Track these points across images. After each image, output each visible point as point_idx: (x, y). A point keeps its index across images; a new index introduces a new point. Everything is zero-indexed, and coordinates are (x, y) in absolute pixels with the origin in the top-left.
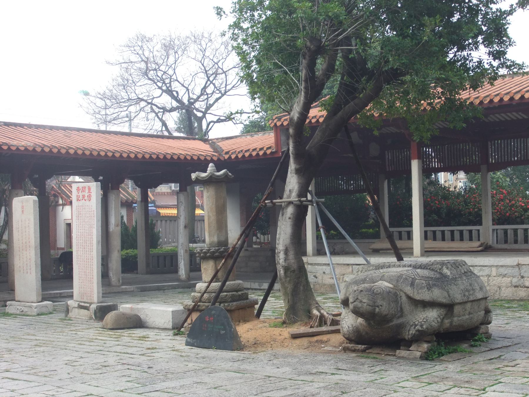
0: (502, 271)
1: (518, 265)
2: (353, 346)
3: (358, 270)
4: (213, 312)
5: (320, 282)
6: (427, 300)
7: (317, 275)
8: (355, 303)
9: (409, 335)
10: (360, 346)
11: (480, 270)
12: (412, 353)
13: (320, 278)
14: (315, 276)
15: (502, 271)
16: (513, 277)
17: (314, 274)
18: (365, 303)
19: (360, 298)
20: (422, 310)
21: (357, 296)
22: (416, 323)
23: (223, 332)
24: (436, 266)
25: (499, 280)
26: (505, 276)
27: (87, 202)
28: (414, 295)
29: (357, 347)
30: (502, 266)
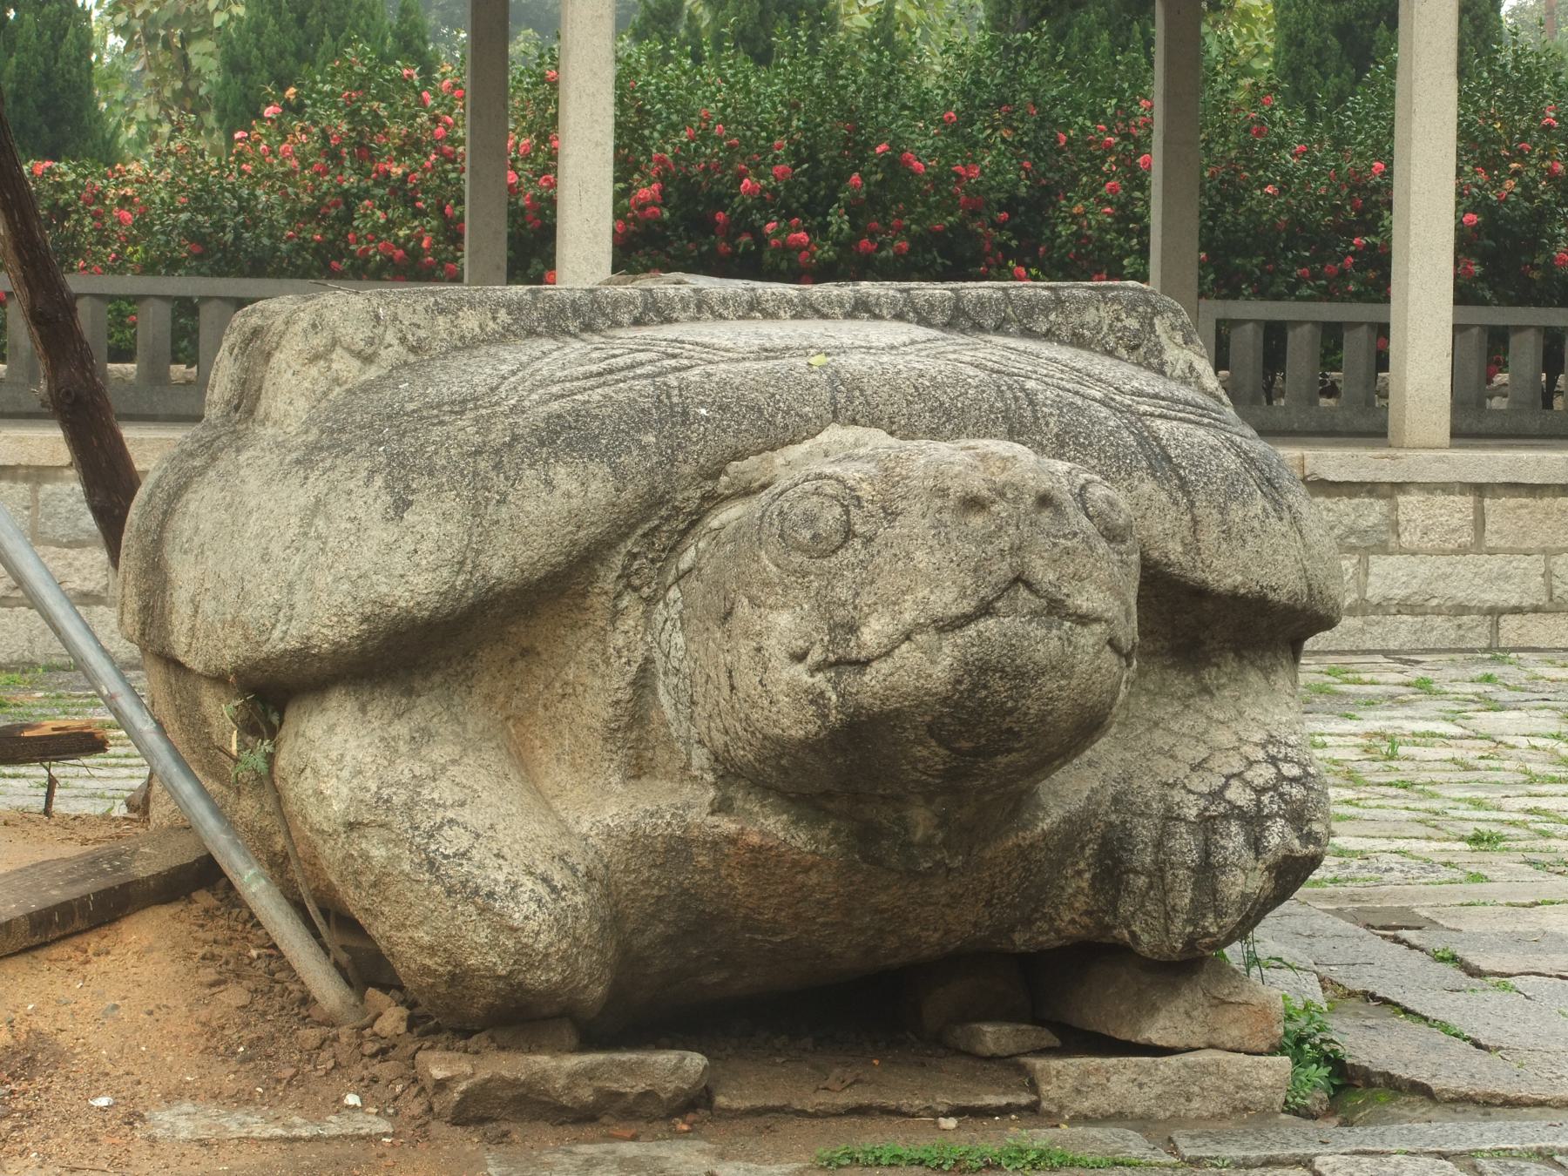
2: (590, 1073)
3: (319, 341)
6: (1282, 597)
8: (989, 625)
9: (1197, 910)
10: (665, 1059)
12: (1204, 1069)
18: (1084, 619)
19: (1044, 574)
20: (1180, 683)
21: (1016, 550)
22: (1238, 795)
24: (1090, 316)
28: (1193, 548)
29: (630, 1070)
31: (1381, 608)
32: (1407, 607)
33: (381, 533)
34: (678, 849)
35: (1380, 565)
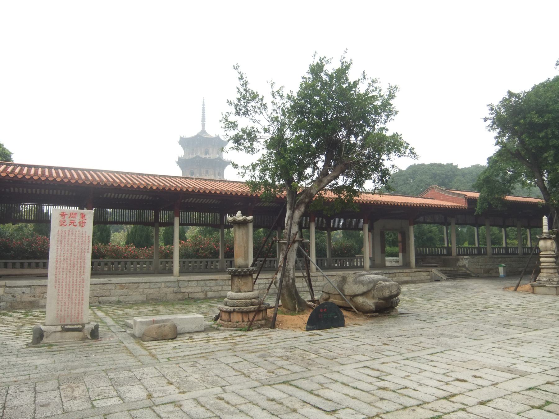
0: (168, 284)
1: (178, 281)
4: (326, 306)
5: (19, 300)
7: (16, 295)
11: (155, 285)
13: (19, 297)
14: (13, 296)
15: (168, 284)
16: (174, 288)
17: (12, 294)
23: (335, 317)
25: (166, 290)
26: (169, 287)
27: (79, 228)
30: (168, 282)
31: (317, 286)
32: (318, 286)
33: (363, 288)
34: (377, 303)
35: (316, 283)
